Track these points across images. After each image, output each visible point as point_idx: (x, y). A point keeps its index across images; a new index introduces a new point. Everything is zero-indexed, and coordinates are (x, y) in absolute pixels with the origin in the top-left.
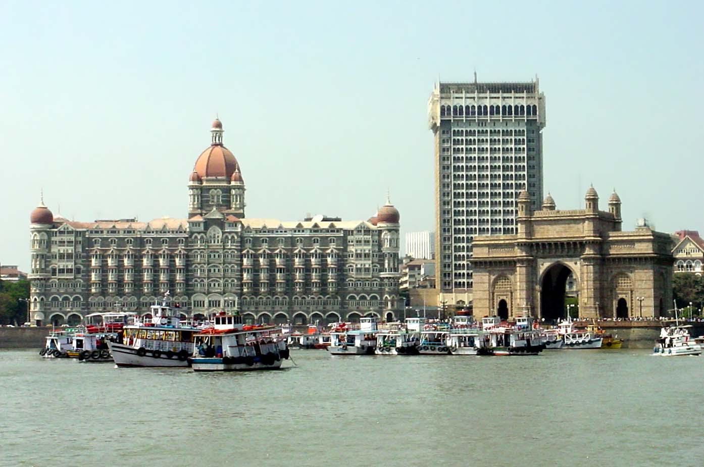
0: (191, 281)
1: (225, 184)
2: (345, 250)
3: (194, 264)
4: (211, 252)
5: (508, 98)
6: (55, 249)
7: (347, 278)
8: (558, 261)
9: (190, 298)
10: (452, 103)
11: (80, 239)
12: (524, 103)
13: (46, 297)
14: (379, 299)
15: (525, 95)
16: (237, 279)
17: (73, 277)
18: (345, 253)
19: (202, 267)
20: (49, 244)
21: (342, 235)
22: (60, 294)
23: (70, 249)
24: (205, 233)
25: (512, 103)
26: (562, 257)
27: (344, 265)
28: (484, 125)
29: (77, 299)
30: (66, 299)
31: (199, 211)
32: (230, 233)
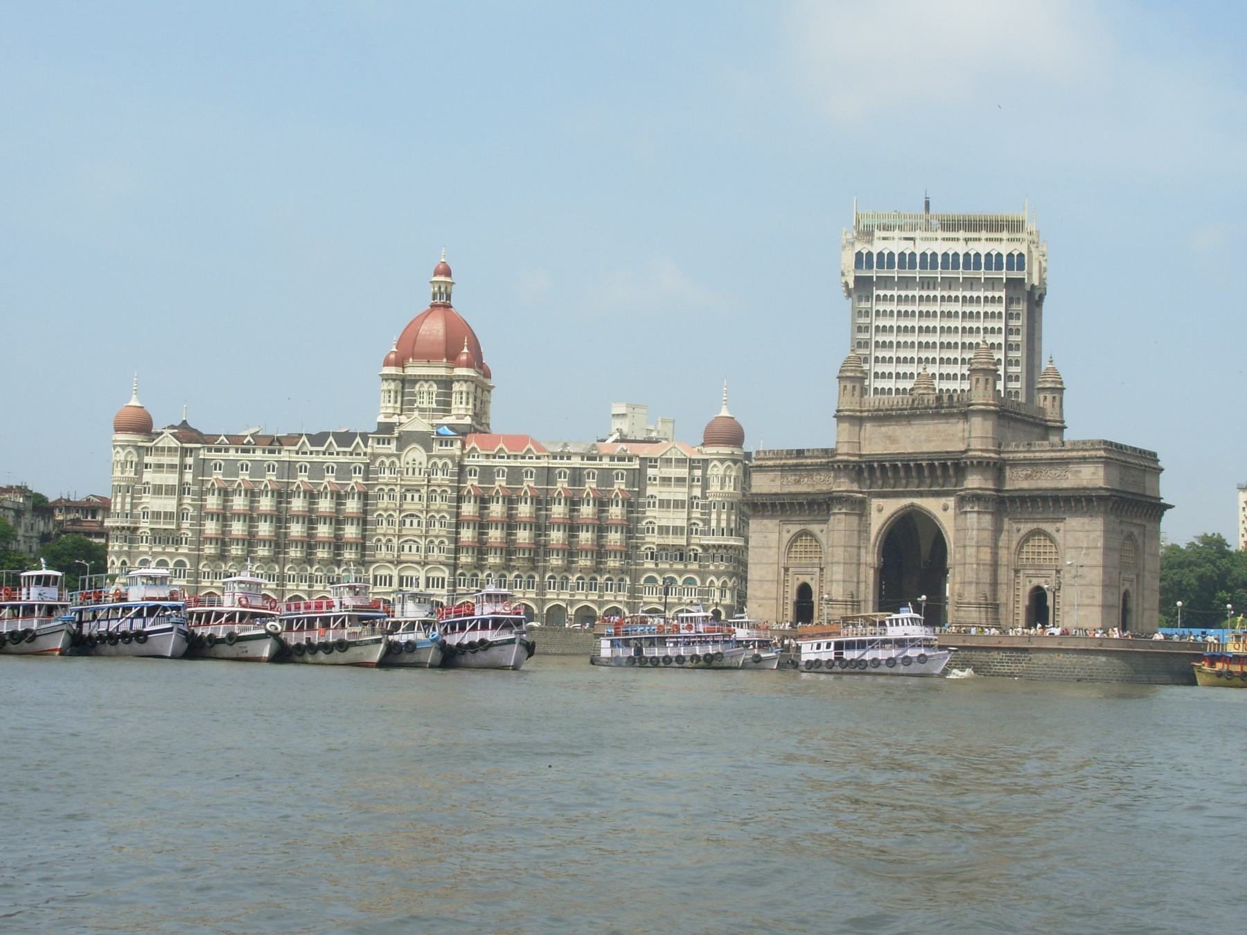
1: (442, 372)
2: (641, 493)
3: (377, 510)
4: (408, 490)
5: (975, 239)
7: (643, 544)
8: (912, 505)
9: (367, 571)
10: (877, 247)
11: (189, 460)
12: (1004, 249)
13: (129, 557)
14: (699, 583)
15: (1005, 235)
16: (448, 538)
17: (173, 527)
18: (641, 500)
19: (391, 515)
21: (638, 467)
23: (172, 479)
24: (399, 457)
25: (983, 248)
26: (920, 494)
27: (639, 520)
28: (931, 286)
32: (440, 457)
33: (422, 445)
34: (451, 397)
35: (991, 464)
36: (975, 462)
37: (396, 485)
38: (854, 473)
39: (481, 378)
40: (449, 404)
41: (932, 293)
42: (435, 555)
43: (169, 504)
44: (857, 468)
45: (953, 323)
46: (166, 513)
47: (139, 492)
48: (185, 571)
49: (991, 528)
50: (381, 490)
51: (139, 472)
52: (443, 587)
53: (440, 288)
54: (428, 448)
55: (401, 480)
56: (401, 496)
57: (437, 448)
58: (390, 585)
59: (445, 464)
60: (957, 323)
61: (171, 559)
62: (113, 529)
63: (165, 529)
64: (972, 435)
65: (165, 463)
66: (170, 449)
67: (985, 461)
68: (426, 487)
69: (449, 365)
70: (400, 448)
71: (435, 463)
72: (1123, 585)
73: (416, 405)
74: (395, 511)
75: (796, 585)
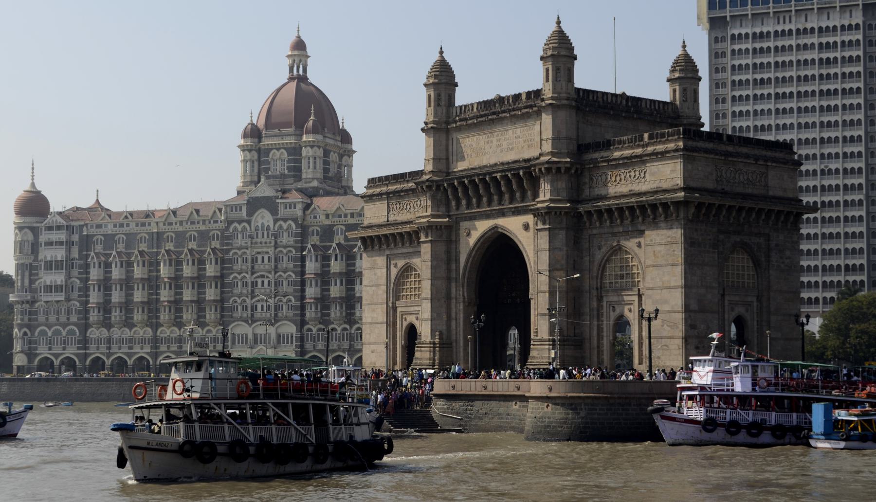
0: (228, 301)
1: (292, 140)
3: (232, 273)
6: (47, 254)
8: (495, 228)
13: (30, 331)
16: (294, 297)
17: (62, 298)
19: (244, 277)
20: (35, 248)
22: (49, 328)
23: (60, 254)
24: (249, 222)
26: (502, 214)
29: (71, 332)
30: (57, 333)
31: (252, 187)
33: (267, 210)
34: (301, 163)
35: (563, 171)
36: (543, 169)
37: (247, 249)
38: (440, 194)
39: (339, 144)
40: (299, 169)
41: (787, 28)
42: (284, 312)
43: (58, 278)
44: (442, 188)
45: (809, 56)
46: (56, 286)
47: (36, 268)
48: (75, 338)
49: (565, 249)
50: (235, 253)
51: (35, 248)
52: (292, 343)
53: (294, 61)
54: (274, 211)
55: (252, 243)
56: (252, 260)
57: (282, 212)
58: (246, 343)
59: (290, 226)
60: (814, 55)
61: (64, 330)
62: (18, 302)
63: (57, 302)
64: (544, 137)
65: (54, 240)
66: (59, 228)
67: (555, 166)
68: (273, 249)
69: (298, 132)
70: (250, 213)
71: (281, 226)
72: (733, 310)
73: (270, 173)
74: (247, 273)
75: (405, 324)
